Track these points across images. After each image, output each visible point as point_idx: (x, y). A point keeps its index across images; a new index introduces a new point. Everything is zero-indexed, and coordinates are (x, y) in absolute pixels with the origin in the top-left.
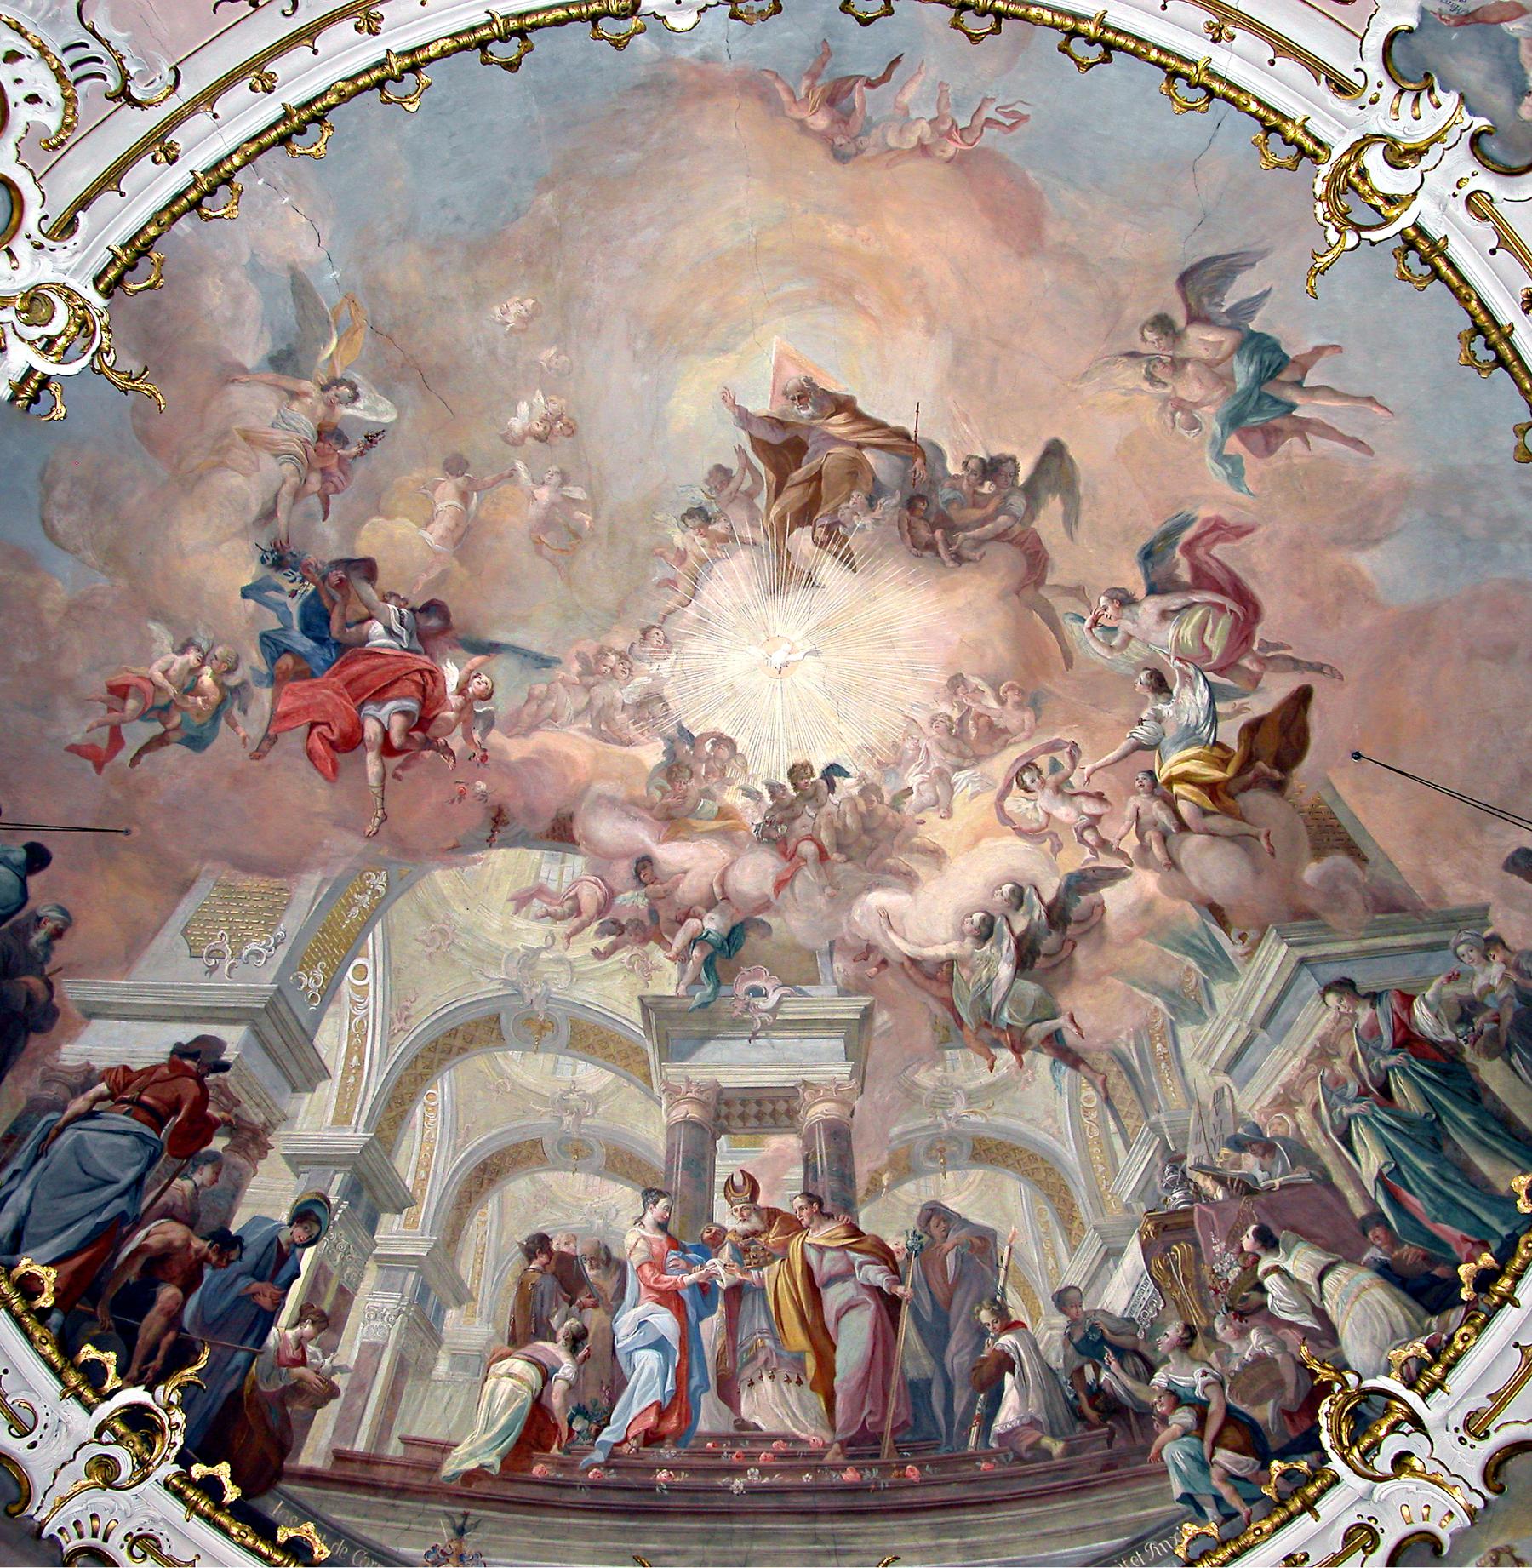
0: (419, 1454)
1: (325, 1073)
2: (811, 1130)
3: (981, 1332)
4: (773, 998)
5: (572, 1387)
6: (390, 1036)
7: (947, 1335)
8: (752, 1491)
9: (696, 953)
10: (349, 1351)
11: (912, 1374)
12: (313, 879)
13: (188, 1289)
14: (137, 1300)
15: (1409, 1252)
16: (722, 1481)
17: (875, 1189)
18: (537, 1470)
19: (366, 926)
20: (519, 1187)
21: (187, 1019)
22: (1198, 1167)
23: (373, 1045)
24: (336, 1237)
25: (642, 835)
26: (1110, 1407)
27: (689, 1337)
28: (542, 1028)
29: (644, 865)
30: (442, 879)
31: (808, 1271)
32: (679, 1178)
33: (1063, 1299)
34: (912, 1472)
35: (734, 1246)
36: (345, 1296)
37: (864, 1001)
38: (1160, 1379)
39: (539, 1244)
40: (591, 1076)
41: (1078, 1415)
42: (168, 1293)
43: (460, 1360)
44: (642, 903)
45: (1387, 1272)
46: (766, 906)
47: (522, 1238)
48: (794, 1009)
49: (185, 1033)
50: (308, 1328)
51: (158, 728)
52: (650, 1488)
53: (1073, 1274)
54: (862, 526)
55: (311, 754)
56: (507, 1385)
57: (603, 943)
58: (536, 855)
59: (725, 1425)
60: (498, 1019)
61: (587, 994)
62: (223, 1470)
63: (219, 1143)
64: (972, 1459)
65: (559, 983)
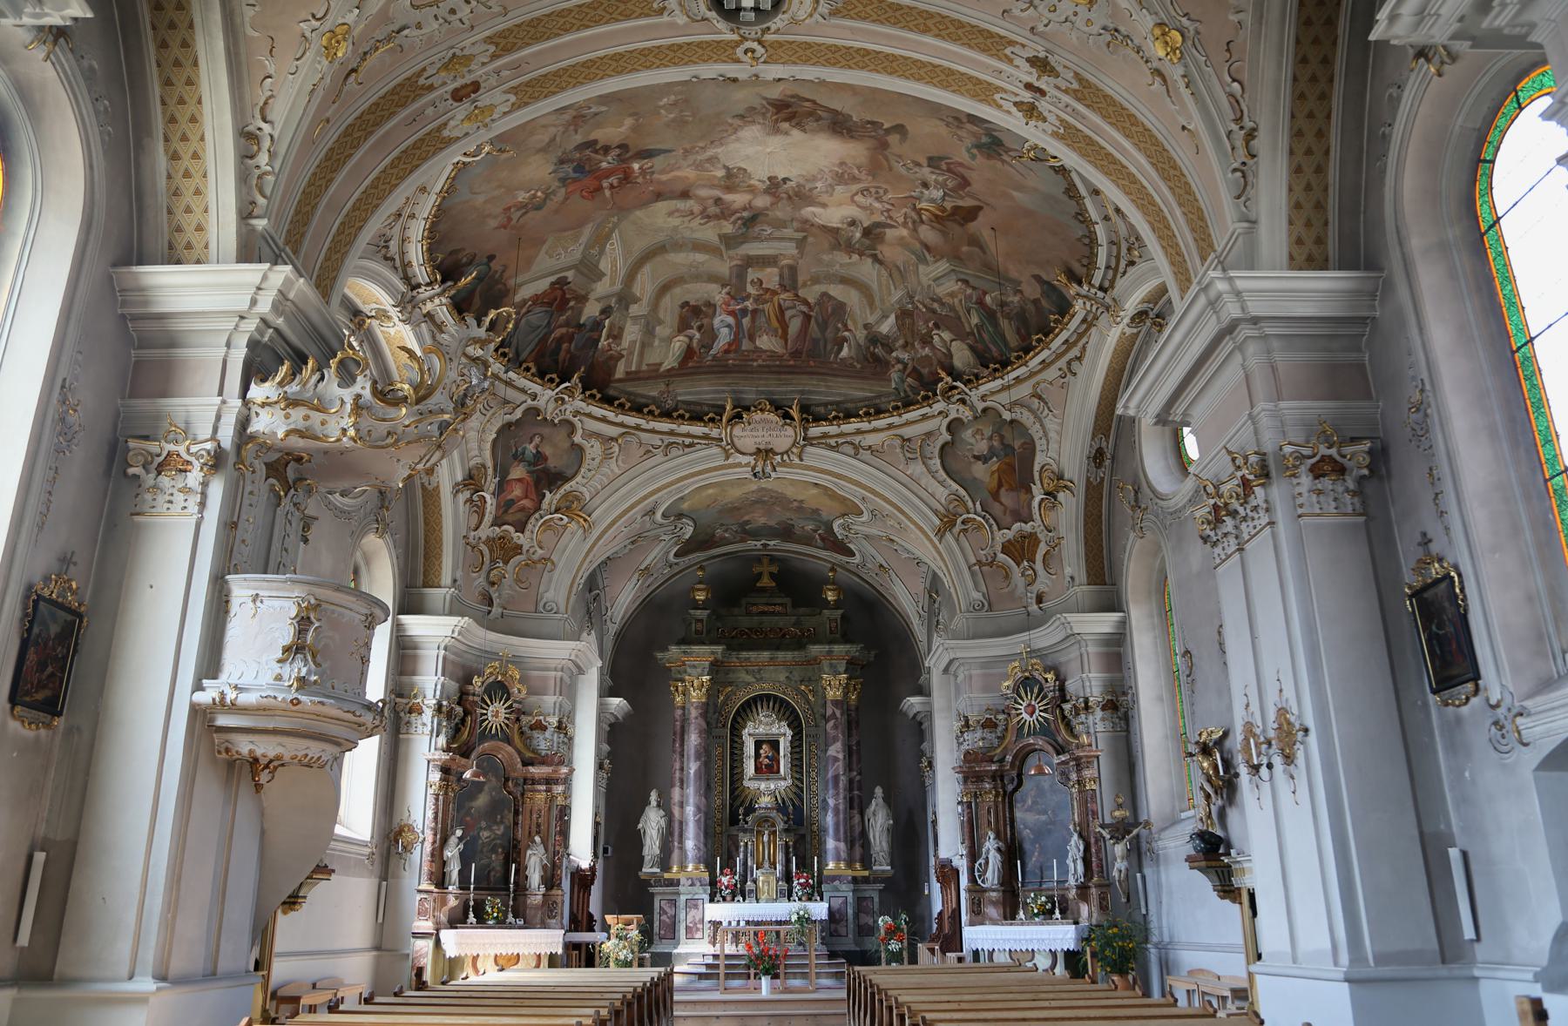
0: (652, 368)
1: (604, 275)
2: (782, 267)
3: (838, 330)
4: (769, 232)
5: (699, 341)
6: (625, 260)
7: (826, 329)
8: (760, 366)
9: (739, 222)
10: (625, 343)
11: (814, 336)
12: (591, 224)
13: (570, 343)
15: (979, 346)
16: (750, 363)
17: (805, 285)
18: (690, 365)
19: (612, 231)
20: (677, 291)
21: (553, 274)
22: (919, 301)
24: (615, 316)
25: (717, 193)
26: (877, 359)
27: (739, 324)
28: (681, 246)
29: (718, 201)
30: (638, 213)
31: (780, 305)
32: (734, 281)
33: (866, 326)
34: (812, 363)
35: (754, 299)
36: (621, 329)
37: (805, 234)
38: (894, 354)
39: (686, 304)
40: (700, 257)
42: (565, 346)
43: (662, 340)
44: (718, 210)
45: (972, 348)
46: (767, 209)
47: (680, 303)
48: (777, 234)
49: (553, 279)
50: (611, 340)
51: (524, 210)
52: (726, 366)
53: (871, 319)
54: (812, 125)
55: (583, 197)
56: (678, 344)
57: (702, 222)
58: (674, 202)
59: (751, 347)
60: (664, 246)
61: (698, 235)
62: (594, 391)
63: (572, 303)
64: (831, 363)
65: (687, 234)
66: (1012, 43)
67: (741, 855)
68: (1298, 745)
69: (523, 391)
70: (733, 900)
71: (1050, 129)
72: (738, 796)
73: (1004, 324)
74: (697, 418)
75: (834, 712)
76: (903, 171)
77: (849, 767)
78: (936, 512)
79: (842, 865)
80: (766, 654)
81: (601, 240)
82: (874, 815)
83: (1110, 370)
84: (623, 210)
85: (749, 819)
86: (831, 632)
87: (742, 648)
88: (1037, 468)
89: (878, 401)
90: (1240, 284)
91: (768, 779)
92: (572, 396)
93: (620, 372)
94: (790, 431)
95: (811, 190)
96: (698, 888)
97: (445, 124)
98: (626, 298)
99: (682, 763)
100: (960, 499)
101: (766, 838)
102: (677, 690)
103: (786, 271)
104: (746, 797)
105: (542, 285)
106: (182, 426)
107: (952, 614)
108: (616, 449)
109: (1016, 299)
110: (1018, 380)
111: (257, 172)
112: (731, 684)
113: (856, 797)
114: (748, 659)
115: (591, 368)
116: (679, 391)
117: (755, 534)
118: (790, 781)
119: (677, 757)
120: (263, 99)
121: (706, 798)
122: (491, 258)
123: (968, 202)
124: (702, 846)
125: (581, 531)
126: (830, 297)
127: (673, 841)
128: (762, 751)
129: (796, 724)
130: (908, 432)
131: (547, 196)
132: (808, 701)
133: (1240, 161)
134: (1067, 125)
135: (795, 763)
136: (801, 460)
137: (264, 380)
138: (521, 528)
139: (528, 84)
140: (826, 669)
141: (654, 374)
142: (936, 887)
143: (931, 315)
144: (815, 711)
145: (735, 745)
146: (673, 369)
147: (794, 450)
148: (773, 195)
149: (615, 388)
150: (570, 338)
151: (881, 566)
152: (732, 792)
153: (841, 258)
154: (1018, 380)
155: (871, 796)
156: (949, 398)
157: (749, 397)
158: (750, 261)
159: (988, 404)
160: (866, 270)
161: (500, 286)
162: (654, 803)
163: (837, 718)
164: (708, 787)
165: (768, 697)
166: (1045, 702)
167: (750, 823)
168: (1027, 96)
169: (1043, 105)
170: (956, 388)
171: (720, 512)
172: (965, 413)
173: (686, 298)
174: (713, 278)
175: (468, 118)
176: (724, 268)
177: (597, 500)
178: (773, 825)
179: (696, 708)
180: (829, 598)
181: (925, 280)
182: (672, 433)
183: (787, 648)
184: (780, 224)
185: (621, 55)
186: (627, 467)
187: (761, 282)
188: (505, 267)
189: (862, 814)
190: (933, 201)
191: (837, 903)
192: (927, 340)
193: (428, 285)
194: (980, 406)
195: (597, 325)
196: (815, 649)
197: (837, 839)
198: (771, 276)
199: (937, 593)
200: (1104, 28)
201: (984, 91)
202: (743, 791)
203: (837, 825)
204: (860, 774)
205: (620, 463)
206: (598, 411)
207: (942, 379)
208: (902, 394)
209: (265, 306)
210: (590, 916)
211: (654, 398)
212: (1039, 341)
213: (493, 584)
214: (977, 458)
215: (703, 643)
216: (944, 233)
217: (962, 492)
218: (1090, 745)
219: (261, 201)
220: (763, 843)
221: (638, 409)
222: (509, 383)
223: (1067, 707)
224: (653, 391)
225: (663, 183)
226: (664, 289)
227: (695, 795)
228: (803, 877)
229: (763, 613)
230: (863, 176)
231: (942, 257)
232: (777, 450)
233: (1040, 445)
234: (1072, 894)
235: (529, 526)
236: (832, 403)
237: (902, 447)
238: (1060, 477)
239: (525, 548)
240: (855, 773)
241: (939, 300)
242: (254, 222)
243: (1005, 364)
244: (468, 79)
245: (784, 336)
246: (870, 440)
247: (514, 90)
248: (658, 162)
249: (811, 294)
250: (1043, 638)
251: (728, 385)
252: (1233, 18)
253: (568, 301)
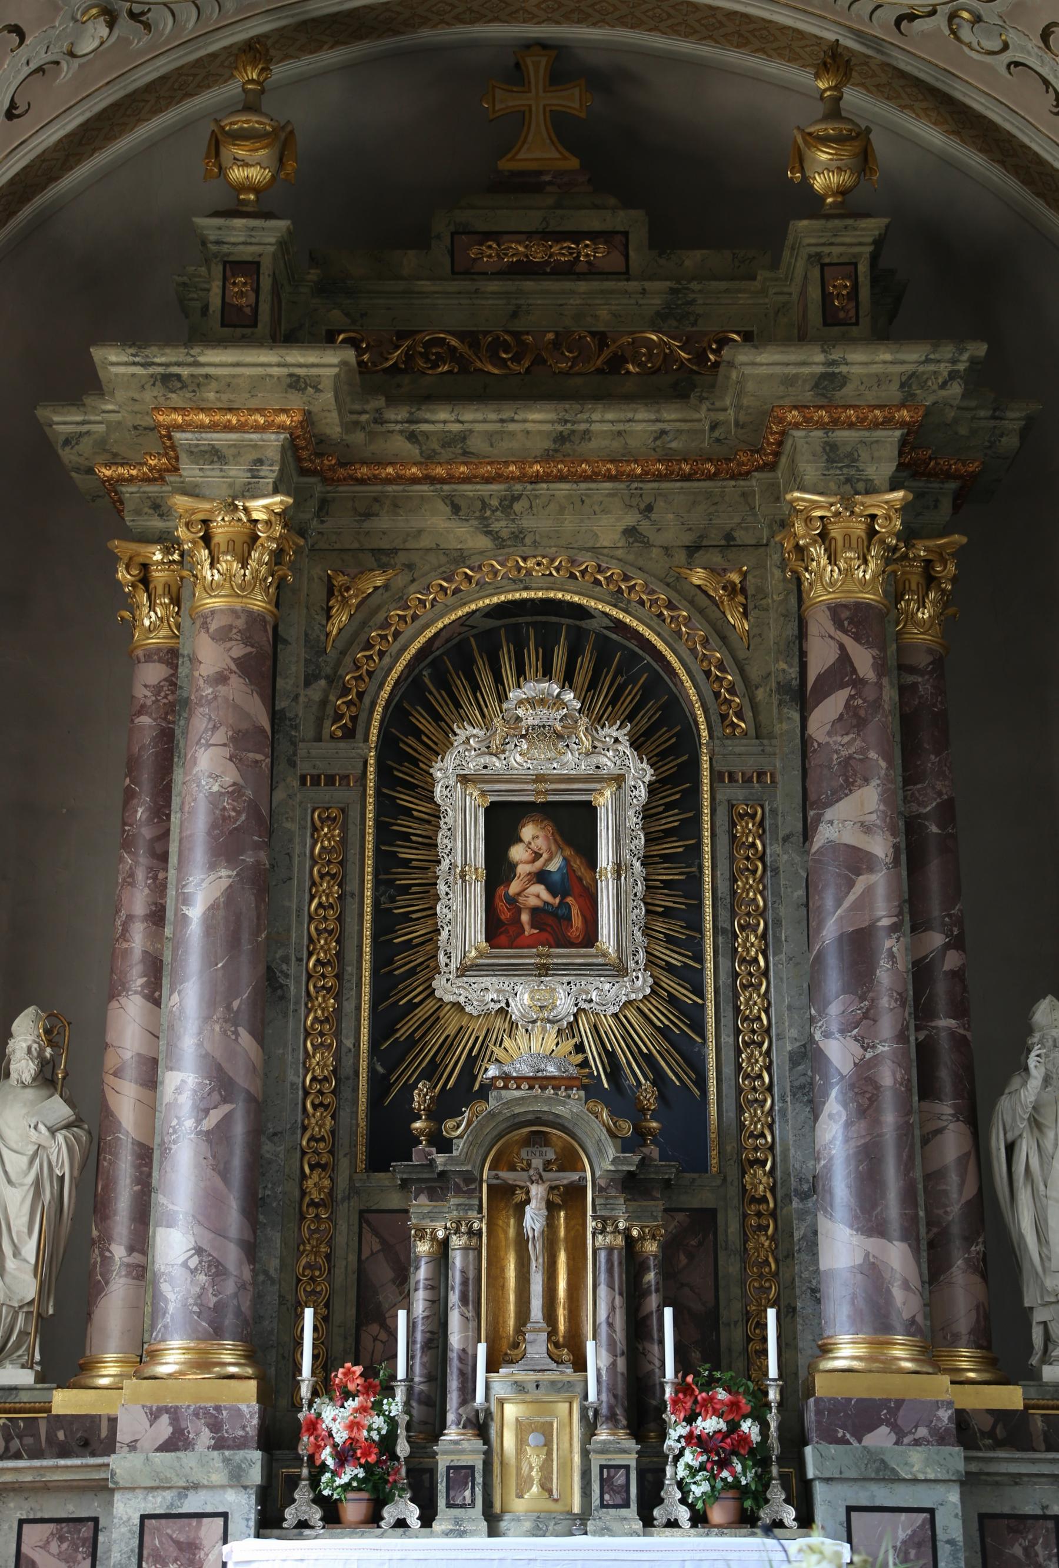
67: (420, 1301)
70: (374, 1519)
72: (411, 1042)
75: (844, 658)
82: (1036, 1124)
85: (451, 1128)
91: (544, 970)
99: (160, 888)
101: (534, 1219)
102: (145, 581)
104: (448, 1046)
112: (383, 557)
113: (944, 1044)
118: (640, 984)
119: (137, 862)
121: (259, 1036)
124: (232, 1256)
127: (105, 1239)
128: (517, 853)
129: (665, 737)
132: (722, 633)
140: (810, 471)
144: (754, 673)
145: (402, 825)
152: (383, 1027)
162: (22, 1067)
163: (858, 683)
167: (459, 1147)
178: (569, 1161)
179: (222, 636)
180: (819, 183)
202: (434, 1020)
204: (957, 943)
220: (522, 1242)
227: (207, 1019)
228: (709, 1407)
229: (523, 269)
240: (937, 939)
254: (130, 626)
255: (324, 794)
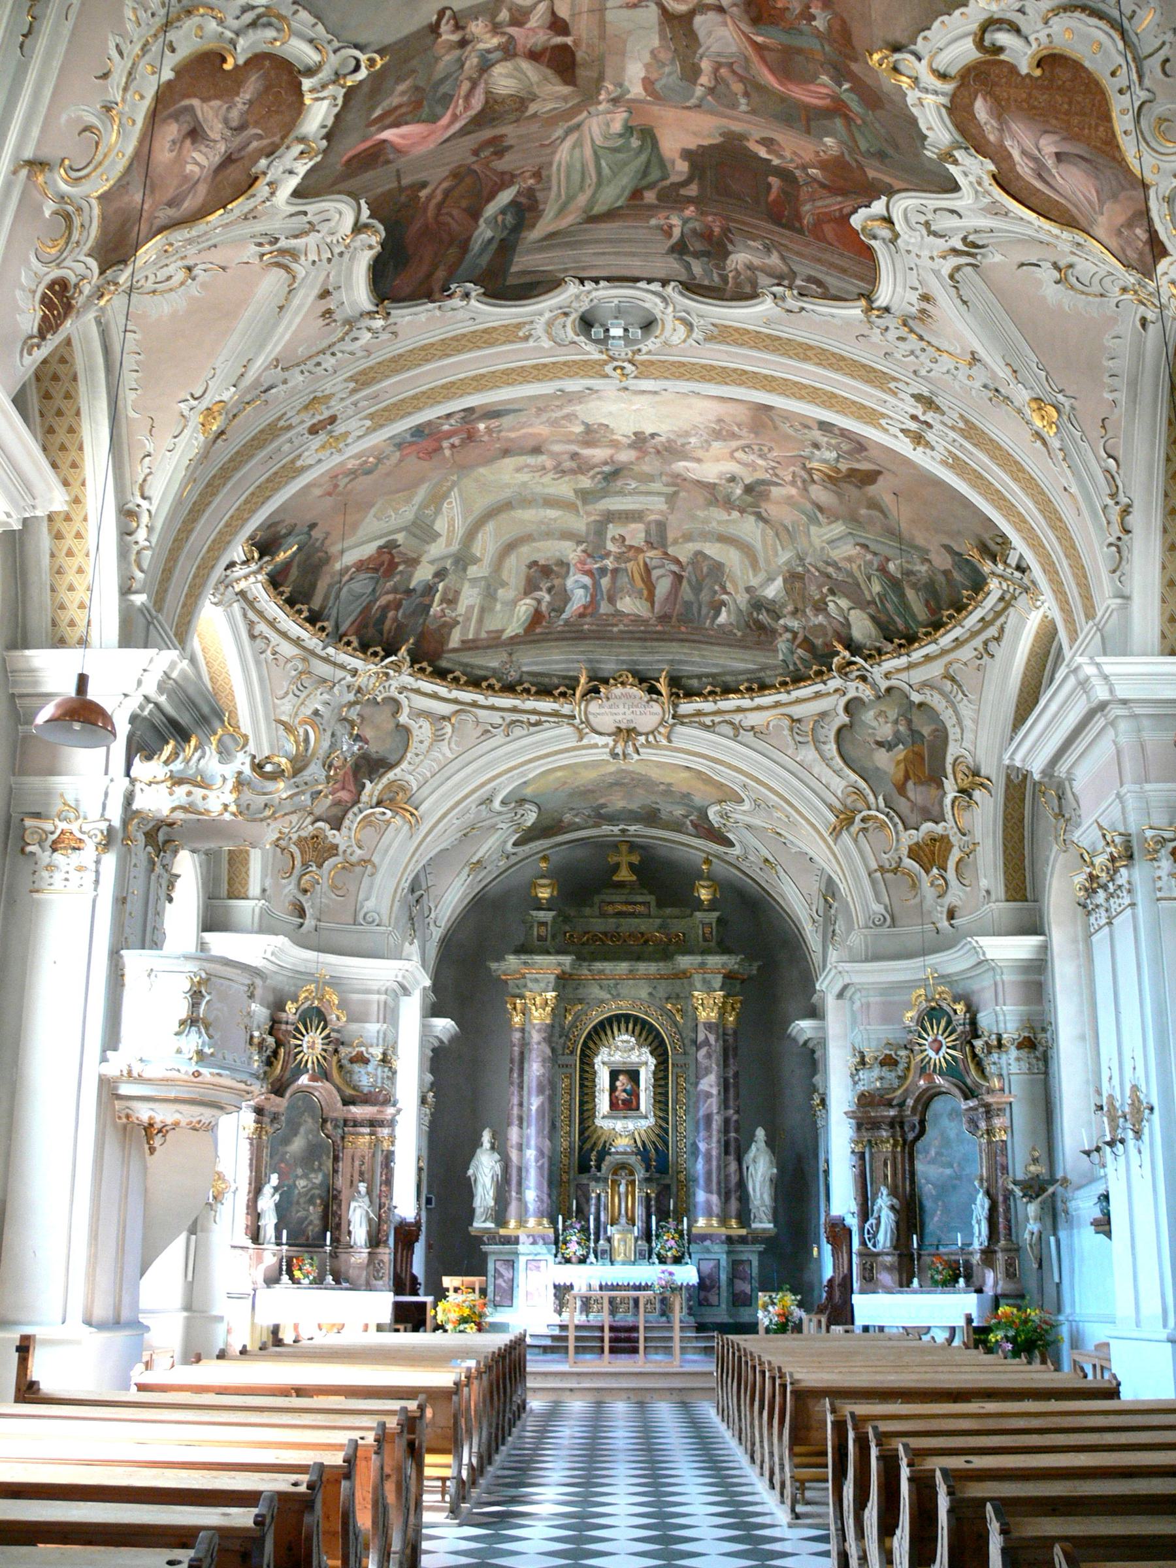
1: (439, 535)
3: (715, 592)
6: (465, 518)
8: (621, 632)
10: (462, 608)
14: (382, 619)
15: (883, 618)
17: (675, 542)
19: (450, 489)
23: (459, 522)
24: (451, 579)
26: (761, 627)
27: (596, 584)
29: (574, 456)
30: (482, 470)
31: (646, 565)
32: (591, 538)
33: (748, 590)
34: (683, 629)
36: (457, 593)
38: (782, 622)
39: (535, 563)
40: (552, 513)
41: (748, 626)
42: (391, 614)
43: (505, 604)
45: (873, 618)
47: (527, 562)
49: (381, 542)
53: (754, 582)
56: (524, 608)
59: (610, 610)
61: (551, 490)
62: (424, 664)
63: (401, 568)
65: (538, 489)
66: (895, 379)
68: (1145, 1123)
69: (342, 667)
71: (938, 457)
73: (910, 594)
74: (545, 692)
76: (791, 431)
77: (725, 1104)
78: (830, 807)
79: (715, 1222)
80: (623, 967)
81: (437, 499)
83: (1033, 654)
84: (464, 468)
86: (705, 940)
87: (594, 957)
88: (949, 760)
89: (762, 674)
90: (1107, 669)
92: (398, 670)
93: (455, 640)
94: (656, 708)
95: (683, 445)
96: (541, 1248)
97: (300, 456)
98: (463, 560)
99: (521, 1097)
100: (859, 792)
101: (622, 1189)
102: (515, 1008)
103: (653, 527)
105: (369, 549)
106: (72, 803)
107: (850, 928)
108: (448, 729)
109: (924, 568)
110: (928, 658)
111: (136, 548)
112: (581, 1001)
114: (601, 972)
115: (421, 638)
116: (526, 660)
117: (612, 819)
118: (651, 1121)
120: (142, 477)
121: (550, 1140)
122: (313, 526)
123: (865, 466)
124: (545, 1197)
125: (406, 827)
126: (706, 557)
128: (618, 1084)
129: (660, 1050)
130: (797, 711)
131: (379, 460)
132: (675, 1023)
133: (1115, 536)
134: (956, 458)
135: (659, 1098)
136: (670, 741)
137: (149, 758)
138: (337, 824)
139: (385, 409)
140: (698, 985)
141: (495, 642)
142: (827, 1249)
143: (822, 579)
146: (517, 636)
147: (662, 730)
148: (640, 449)
149: (449, 660)
150: (398, 605)
151: (766, 860)
152: (581, 1133)
153: (718, 515)
154: (928, 658)
155: (751, 1139)
156: (846, 674)
157: (608, 666)
158: (610, 517)
159: (893, 682)
160: (748, 528)
161: (320, 554)
164: (553, 1126)
165: (627, 1017)
166: (953, 1037)
168: (913, 426)
169: (930, 436)
170: (854, 663)
171: (571, 795)
172: (866, 692)
173: (535, 557)
174: (567, 535)
175: (323, 447)
176: (580, 524)
177: (426, 790)
178: (632, 1173)
179: (539, 1031)
181: (817, 542)
182: (514, 710)
183: (650, 960)
184: (650, 478)
185: (483, 376)
186: (461, 750)
187: (623, 538)
188: (328, 534)
189: (739, 1160)
190: (825, 461)
191: (707, 1267)
192: (820, 607)
193: (244, 563)
194: (884, 685)
195: (429, 590)
196: (685, 962)
197: (709, 1191)
198: (635, 534)
199: (833, 897)
200: (985, 386)
201: (871, 416)
203: (709, 1174)
205: (453, 745)
206: (427, 686)
207: (837, 653)
208: (791, 668)
209: (150, 689)
210: (414, 1278)
211: (494, 670)
212: (951, 617)
213: (305, 891)
214: (880, 744)
215: (548, 953)
216: (840, 495)
217: (862, 784)
218: (1002, 1090)
219: (139, 575)
221: (475, 683)
222: (326, 660)
223: (978, 1043)
224: (492, 661)
225: (512, 440)
226: (510, 547)
229: (621, 914)
230: (744, 433)
231: (837, 519)
232: (640, 729)
233: (953, 733)
234: (976, 1259)
235: (346, 823)
236: (707, 676)
237: (791, 729)
238: (976, 774)
239: (341, 849)
241: (835, 565)
242: (133, 597)
243: (911, 639)
244: (326, 414)
245: (651, 599)
246: (753, 719)
247: (371, 417)
248: (506, 421)
249: (684, 552)
250: (952, 962)
251: (583, 652)
252: (1109, 396)
253: (397, 564)
254: (510, 1019)
255: (565, 1070)
